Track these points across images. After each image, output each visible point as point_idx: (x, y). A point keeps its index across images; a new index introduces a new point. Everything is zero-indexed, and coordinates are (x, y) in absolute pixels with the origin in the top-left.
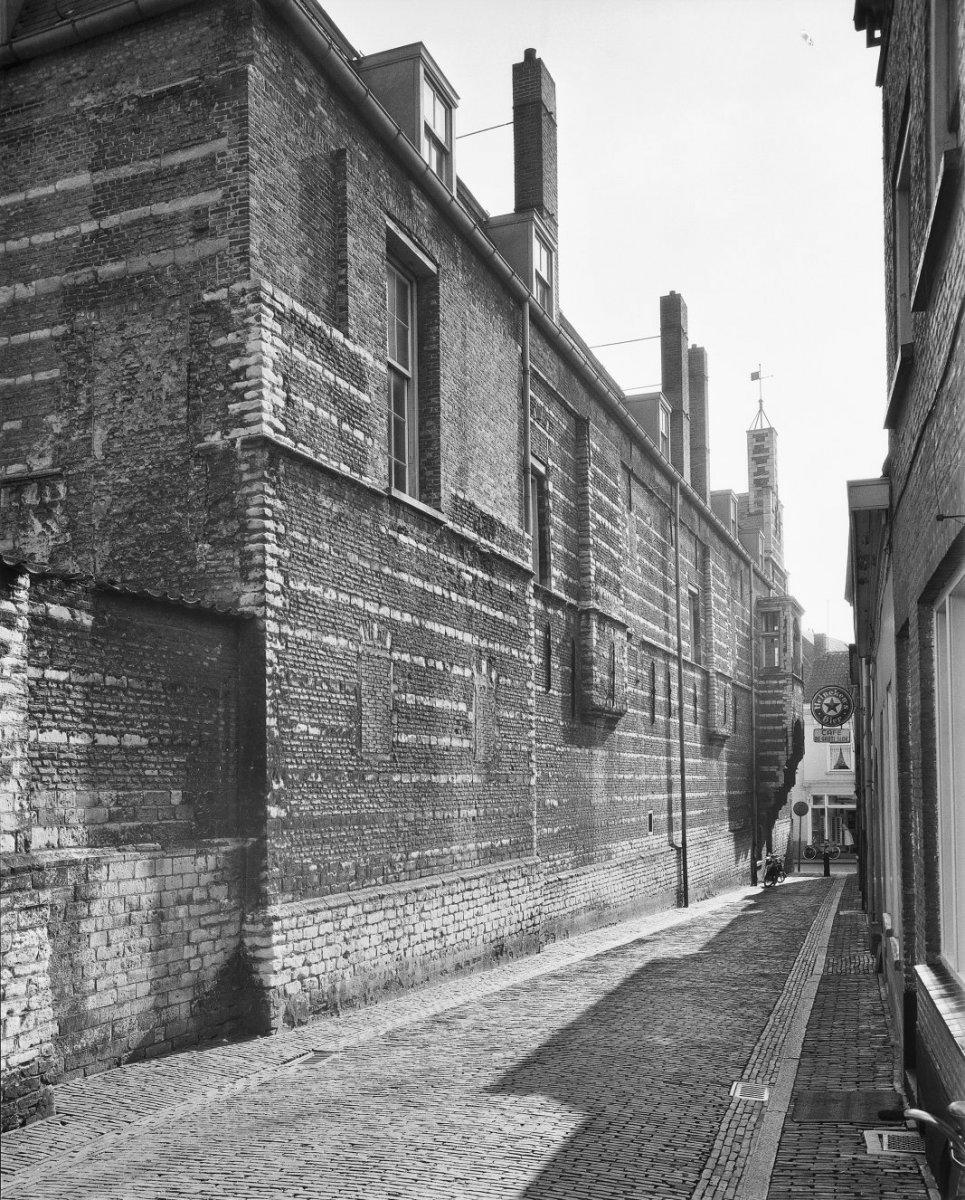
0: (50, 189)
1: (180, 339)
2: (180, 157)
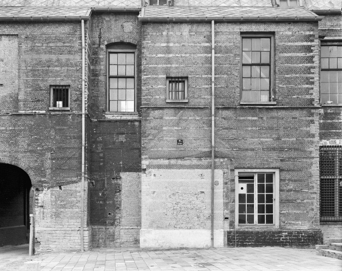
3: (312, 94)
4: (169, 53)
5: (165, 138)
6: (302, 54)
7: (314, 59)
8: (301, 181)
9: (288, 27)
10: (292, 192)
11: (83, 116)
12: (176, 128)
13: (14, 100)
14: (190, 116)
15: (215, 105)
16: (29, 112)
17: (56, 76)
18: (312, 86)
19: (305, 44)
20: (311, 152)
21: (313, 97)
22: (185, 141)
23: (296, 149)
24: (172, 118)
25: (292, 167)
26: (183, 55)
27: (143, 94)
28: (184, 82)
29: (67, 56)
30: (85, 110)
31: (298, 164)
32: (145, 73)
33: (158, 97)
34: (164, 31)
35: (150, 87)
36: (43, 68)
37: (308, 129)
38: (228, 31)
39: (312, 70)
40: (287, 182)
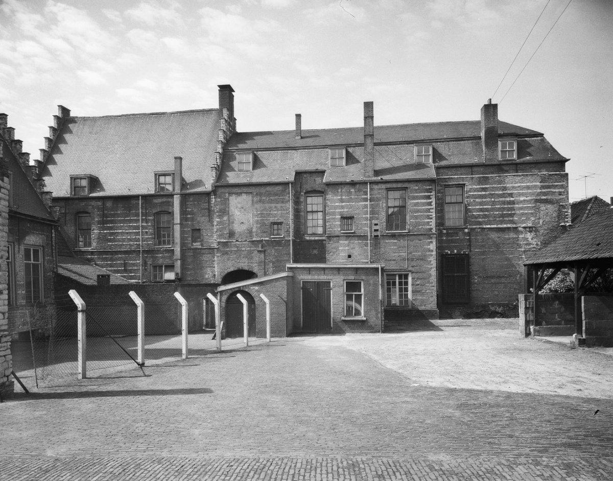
2: (556, 184)
3: (431, 225)
4: (343, 202)
7: (432, 204)
11: (291, 241)
17: (275, 217)
19: (426, 194)
22: (353, 256)
23: (422, 259)
27: (327, 227)
31: (424, 269)
34: (339, 189)
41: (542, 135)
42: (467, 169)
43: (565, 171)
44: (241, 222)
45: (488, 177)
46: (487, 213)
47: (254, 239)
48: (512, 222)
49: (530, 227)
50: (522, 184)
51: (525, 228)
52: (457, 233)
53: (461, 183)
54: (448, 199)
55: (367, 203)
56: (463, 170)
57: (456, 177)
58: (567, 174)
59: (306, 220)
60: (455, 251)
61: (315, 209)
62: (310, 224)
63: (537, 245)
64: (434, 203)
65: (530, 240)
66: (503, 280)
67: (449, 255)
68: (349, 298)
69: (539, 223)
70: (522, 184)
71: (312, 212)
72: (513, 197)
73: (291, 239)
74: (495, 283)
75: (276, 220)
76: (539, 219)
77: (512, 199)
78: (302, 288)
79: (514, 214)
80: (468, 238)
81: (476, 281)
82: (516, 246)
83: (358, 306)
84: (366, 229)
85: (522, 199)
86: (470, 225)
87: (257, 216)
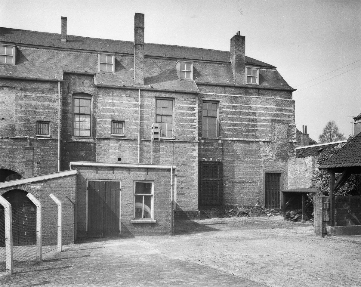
0: (270, 107)
1: (286, 129)
2: (287, 108)
3: (194, 134)
4: (114, 106)
5: (110, 157)
6: (190, 112)
7: (196, 115)
8: (188, 183)
9: (182, 95)
10: (183, 189)
11: (59, 141)
12: (117, 151)
13: (12, 129)
14: (126, 144)
15: (140, 138)
16: (23, 137)
17: (42, 115)
18: (195, 130)
20: (194, 167)
21: (195, 136)
22: (122, 159)
23: (186, 165)
24: (114, 145)
25: (183, 175)
26: (122, 108)
28: (122, 123)
29: (49, 103)
30: (60, 137)
31: (187, 173)
32: (99, 118)
33: (106, 132)
35: (101, 126)
36: (33, 110)
37: (192, 154)
38: (148, 96)
39: (195, 121)
40: (181, 183)
41: (275, 68)
42: (221, 88)
43: (292, 99)
44: (1, 118)
45: (237, 97)
46: (236, 128)
47: (17, 137)
48: (255, 136)
49: (268, 142)
50: (263, 106)
51: (264, 142)
52: (212, 143)
53: (217, 100)
54: (205, 114)
55: (137, 109)
56: (218, 89)
57: (212, 94)
58: (294, 102)
59: (74, 121)
60: (211, 159)
61: (82, 111)
62: (77, 125)
63: (273, 157)
64: (197, 115)
65: (268, 152)
66: (248, 185)
67: (206, 162)
68: (139, 199)
69: (274, 138)
70: (263, 106)
71: (80, 114)
72: (256, 116)
73: (59, 139)
74: (242, 188)
75: (42, 118)
76: (274, 135)
77: (255, 117)
78: (88, 189)
79: (257, 130)
80: (221, 148)
81: (227, 185)
82: (257, 157)
83: (147, 208)
84: (136, 133)
85: (262, 118)
86: (223, 137)
87: (21, 112)
